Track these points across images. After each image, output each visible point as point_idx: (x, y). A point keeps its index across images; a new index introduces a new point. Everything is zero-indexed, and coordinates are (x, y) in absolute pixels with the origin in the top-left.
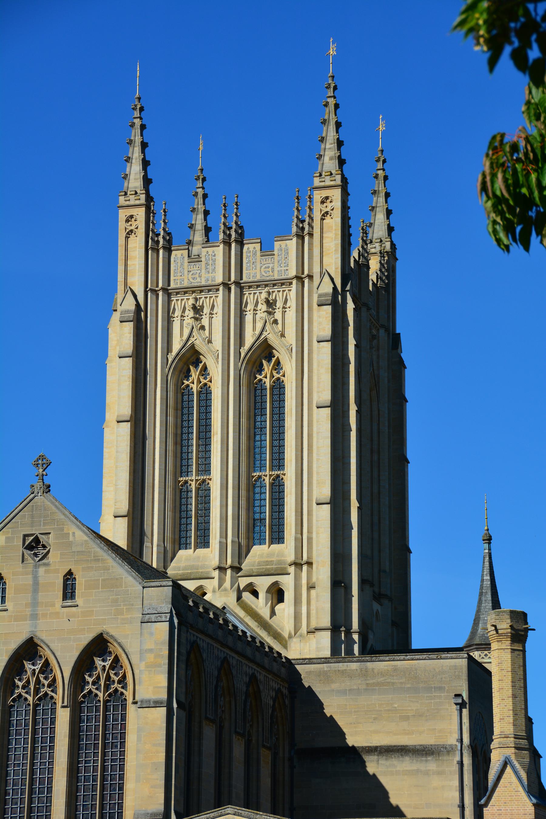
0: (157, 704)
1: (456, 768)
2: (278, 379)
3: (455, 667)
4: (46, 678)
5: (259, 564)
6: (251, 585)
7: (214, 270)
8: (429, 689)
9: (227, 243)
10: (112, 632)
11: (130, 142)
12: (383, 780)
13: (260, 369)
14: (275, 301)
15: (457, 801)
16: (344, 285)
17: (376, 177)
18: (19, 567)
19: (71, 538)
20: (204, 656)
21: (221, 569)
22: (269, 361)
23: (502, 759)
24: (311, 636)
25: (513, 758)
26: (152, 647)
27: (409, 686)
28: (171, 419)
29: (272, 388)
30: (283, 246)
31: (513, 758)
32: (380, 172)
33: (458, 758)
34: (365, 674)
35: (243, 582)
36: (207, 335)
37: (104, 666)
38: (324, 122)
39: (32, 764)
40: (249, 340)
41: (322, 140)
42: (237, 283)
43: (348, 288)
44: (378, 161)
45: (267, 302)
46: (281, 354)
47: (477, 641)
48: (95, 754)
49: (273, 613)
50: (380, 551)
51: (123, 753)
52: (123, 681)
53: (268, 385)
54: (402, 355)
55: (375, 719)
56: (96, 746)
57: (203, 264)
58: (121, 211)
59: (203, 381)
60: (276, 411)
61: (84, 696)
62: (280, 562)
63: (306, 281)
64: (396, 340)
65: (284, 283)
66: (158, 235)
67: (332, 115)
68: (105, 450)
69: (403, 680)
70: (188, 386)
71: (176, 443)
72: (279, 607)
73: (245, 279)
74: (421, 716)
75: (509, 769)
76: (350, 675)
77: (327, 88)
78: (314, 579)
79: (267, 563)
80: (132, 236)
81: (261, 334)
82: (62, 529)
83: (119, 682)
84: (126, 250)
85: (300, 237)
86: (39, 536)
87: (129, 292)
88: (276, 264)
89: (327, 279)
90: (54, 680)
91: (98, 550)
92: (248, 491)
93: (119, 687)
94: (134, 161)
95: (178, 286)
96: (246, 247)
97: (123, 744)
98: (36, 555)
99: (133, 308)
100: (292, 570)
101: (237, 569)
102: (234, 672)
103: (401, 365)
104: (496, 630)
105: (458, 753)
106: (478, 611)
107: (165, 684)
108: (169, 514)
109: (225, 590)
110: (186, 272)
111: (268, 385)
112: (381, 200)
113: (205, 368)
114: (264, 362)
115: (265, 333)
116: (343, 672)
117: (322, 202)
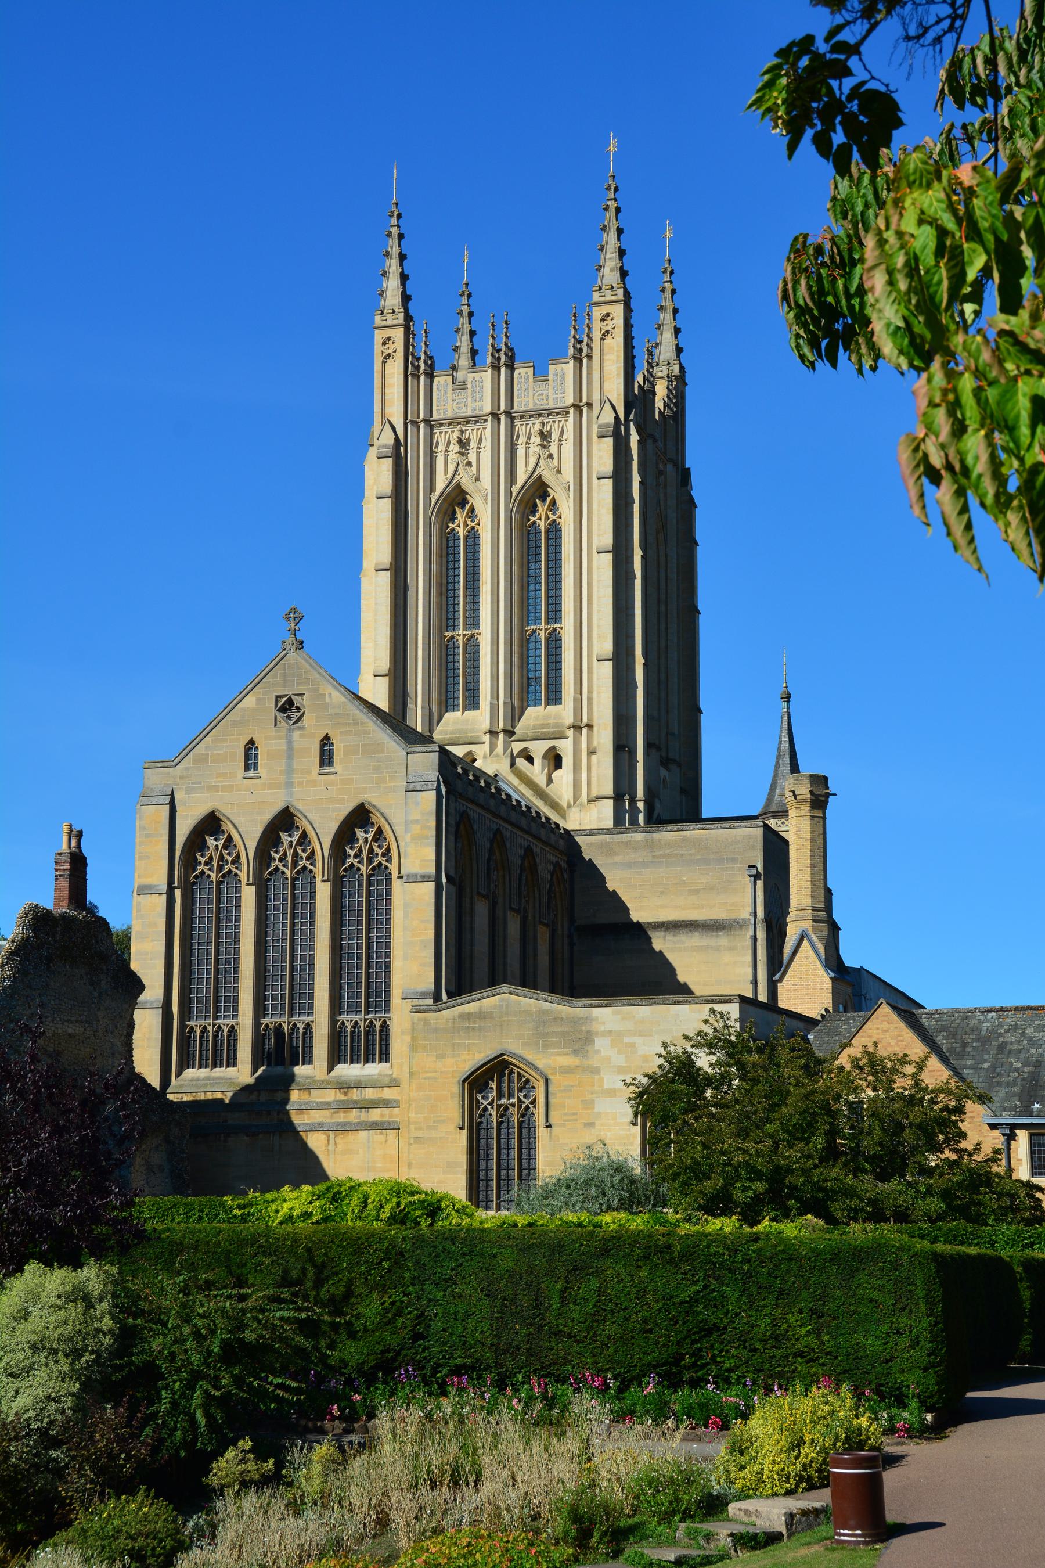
0: (424, 879)
1: (749, 943)
2: (554, 521)
3: (750, 837)
4: (304, 851)
5: (534, 727)
6: (525, 750)
7: (481, 398)
8: (720, 861)
9: (496, 368)
10: (374, 802)
11: (387, 254)
12: (670, 957)
13: (534, 510)
14: (550, 433)
15: (750, 978)
16: (627, 414)
17: (663, 290)
18: (272, 730)
19: (327, 700)
20: (475, 827)
21: (493, 733)
22: (544, 500)
23: (799, 932)
24: (592, 805)
25: (810, 931)
26: (418, 817)
27: (699, 857)
28: (435, 567)
29: (547, 531)
30: (559, 371)
31: (810, 931)
32: (667, 285)
33: (751, 933)
34: (650, 845)
35: (517, 747)
36: (475, 472)
37: (366, 838)
38: (604, 228)
39: (292, 941)
40: (521, 477)
41: (602, 248)
42: (508, 413)
43: (632, 417)
44: (665, 272)
45: (541, 434)
46: (556, 492)
47: (774, 808)
48: (359, 931)
49: (550, 781)
50: (667, 712)
51: (388, 930)
52: (387, 854)
53: (542, 528)
54: (692, 493)
55: (662, 893)
56: (360, 922)
57: (469, 391)
58: (377, 332)
59: (471, 524)
60: (552, 557)
61: (346, 870)
62: (557, 725)
63: (585, 410)
64: (685, 476)
65: (560, 412)
66: (418, 359)
67: (613, 221)
68: (363, 602)
69: (693, 851)
70: (453, 529)
71: (440, 594)
72: (556, 774)
73: (516, 408)
74: (712, 889)
75: (805, 942)
76: (634, 847)
77: (607, 189)
78: (595, 744)
79: (543, 726)
80: (390, 361)
81: (534, 470)
82: (317, 690)
83: (383, 855)
84: (383, 376)
85: (578, 360)
86: (293, 697)
87: (387, 424)
88: (551, 390)
89: (608, 406)
90: (313, 853)
91: (357, 712)
92: (521, 646)
93: (383, 860)
94: (391, 275)
95: (442, 416)
96: (517, 372)
97: (388, 920)
98: (289, 718)
99: (392, 442)
100: (570, 733)
101: (510, 733)
102: (508, 845)
103: (691, 503)
104: (795, 796)
105: (752, 927)
106: (775, 776)
107: (433, 857)
108: (434, 672)
109: (497, 756)
110: (450, 401)
111: (542, 528)
112: (669, 316)
113: (472, 510)
115: (539, 469)
116: (627, 844)
117: (603, 320)
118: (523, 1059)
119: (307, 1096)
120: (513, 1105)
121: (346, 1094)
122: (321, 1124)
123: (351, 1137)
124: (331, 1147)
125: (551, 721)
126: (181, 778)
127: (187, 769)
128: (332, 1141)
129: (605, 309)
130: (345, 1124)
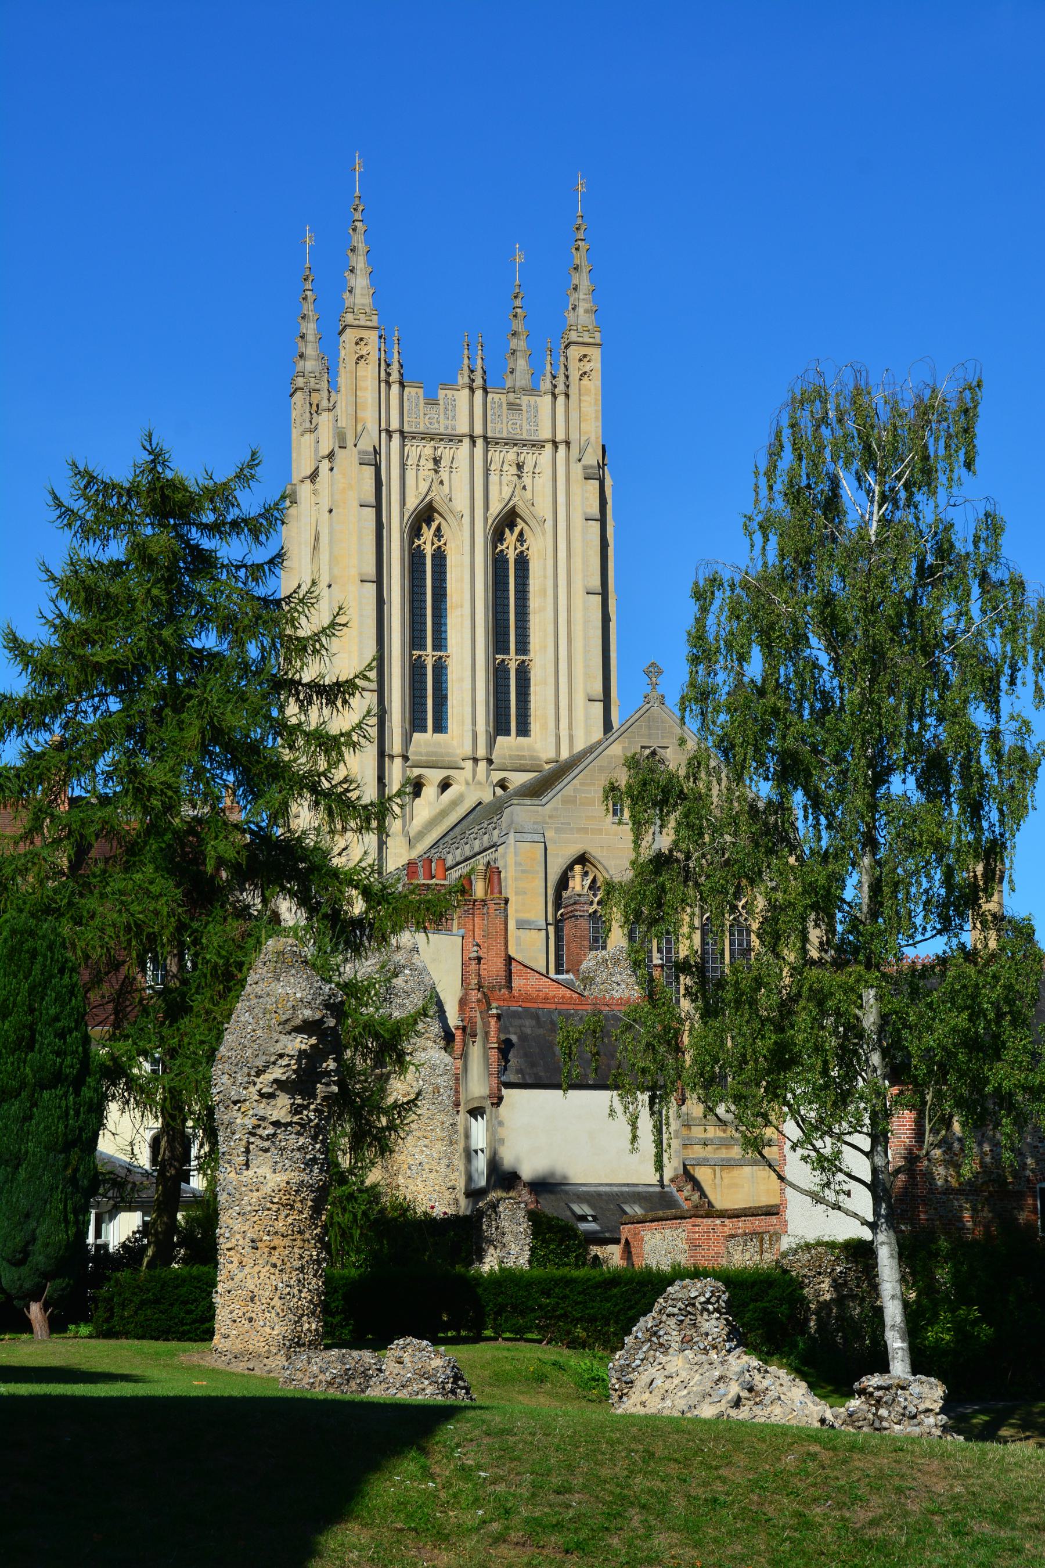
5: (511, 757)
6: (503, 780)
30: (532, 403)
36: (447, 491)
57: (442, 407)
65: (539, 445)
70: (419, 546)
77: (577, 229)
80: (362, 362)
88: (524, 421)
94: (358, 272)
95: (413, 429)
109: (480, 783)
110: (422, 415)
114: (507, 530)
122: (706, 1159)
123: (736, 1172)
124: (718, 1181)
125: (526, 753)
126: (550, 817)
127: (556, 809)
129: (584, 350)
130: (729, 1159)
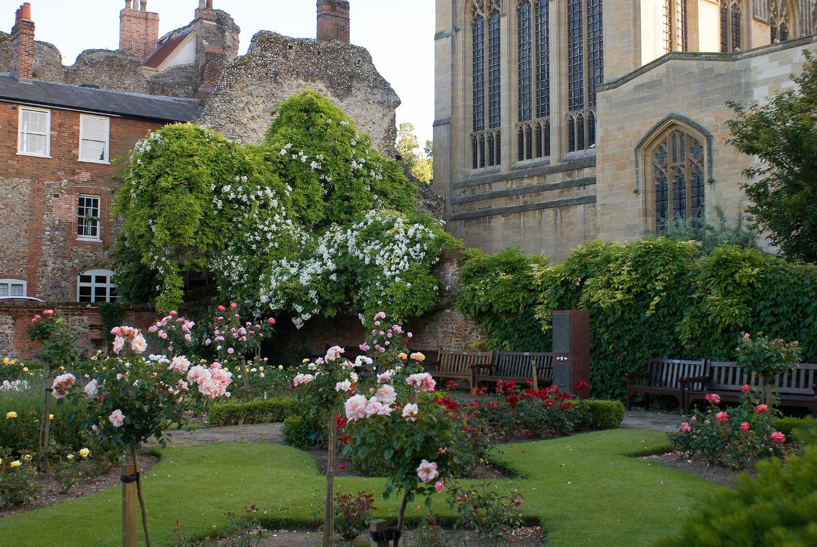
51: (601, 31)
118: (687, 121)
119: (543, 181)
120: (683, 166)
121: (570, 176)
122: (552, 203)
128: (559, 216)
